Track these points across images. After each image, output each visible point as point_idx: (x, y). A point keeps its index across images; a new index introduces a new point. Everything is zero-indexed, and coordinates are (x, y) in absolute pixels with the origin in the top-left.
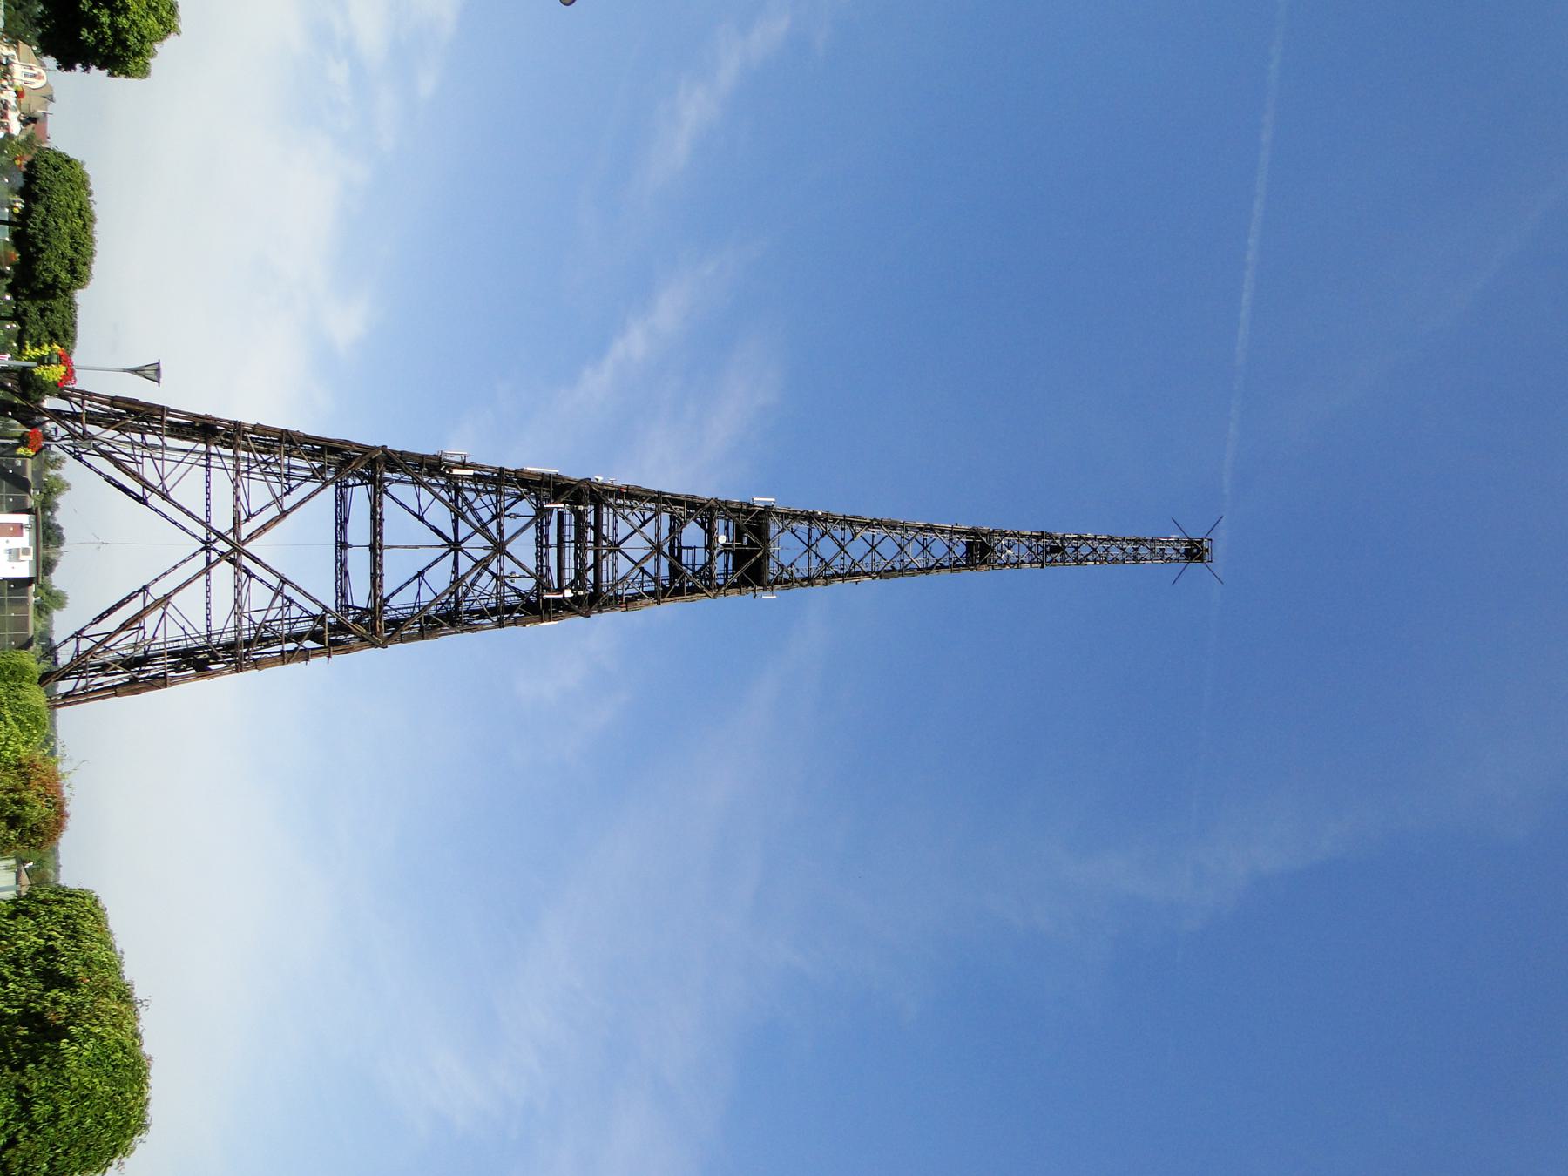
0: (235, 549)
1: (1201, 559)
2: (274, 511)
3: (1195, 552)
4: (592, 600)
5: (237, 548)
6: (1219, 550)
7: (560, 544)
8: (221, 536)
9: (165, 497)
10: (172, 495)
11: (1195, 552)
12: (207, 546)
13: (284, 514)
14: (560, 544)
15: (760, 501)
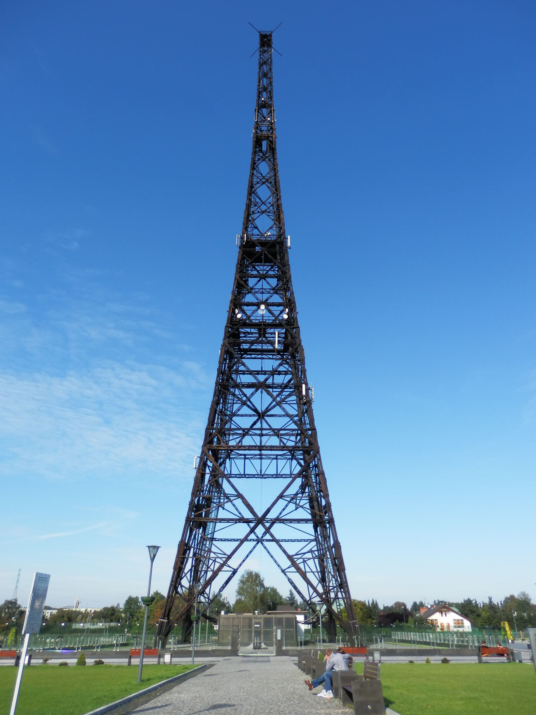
0: (260, 521)
1: (270, 35)
2: (238, 502)
3: (266, 41)
4: (291, 325)
5: (260, 521)
6: (266, 29)
7: (259, 349)
8: (252, 531)
9: (229, 557)
10: (229, 553)
11: (266, 41)
12: (259, 541)
13: (239, 496)
14: (259, 349)
15: (237, 242)
